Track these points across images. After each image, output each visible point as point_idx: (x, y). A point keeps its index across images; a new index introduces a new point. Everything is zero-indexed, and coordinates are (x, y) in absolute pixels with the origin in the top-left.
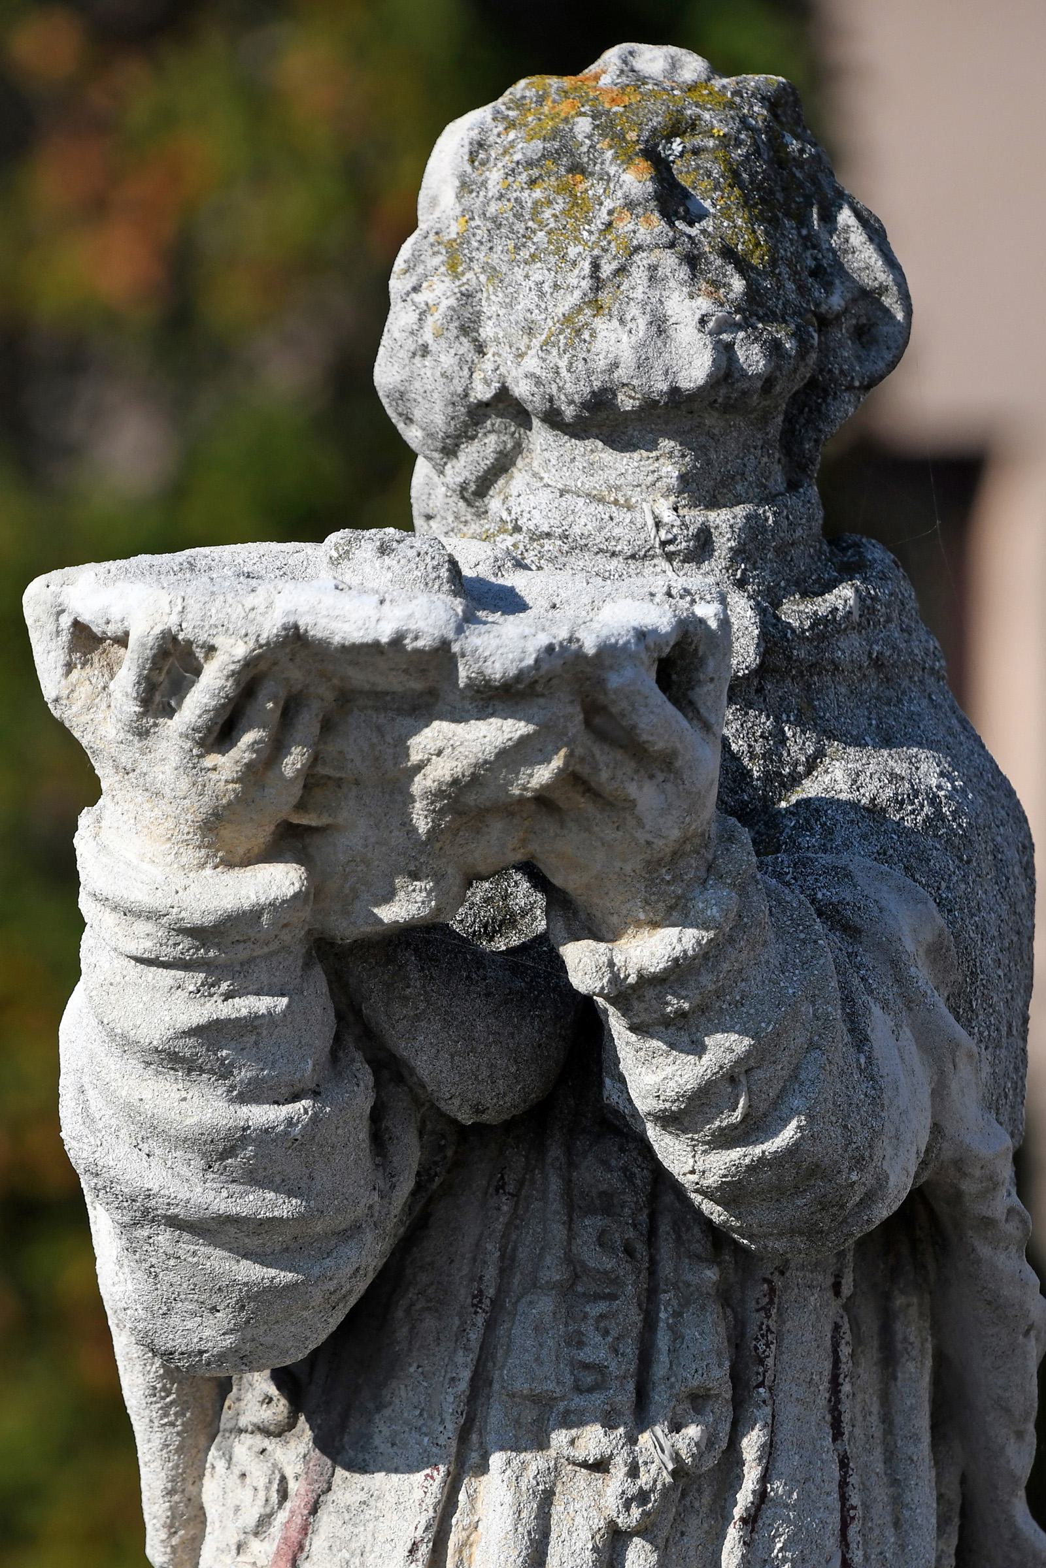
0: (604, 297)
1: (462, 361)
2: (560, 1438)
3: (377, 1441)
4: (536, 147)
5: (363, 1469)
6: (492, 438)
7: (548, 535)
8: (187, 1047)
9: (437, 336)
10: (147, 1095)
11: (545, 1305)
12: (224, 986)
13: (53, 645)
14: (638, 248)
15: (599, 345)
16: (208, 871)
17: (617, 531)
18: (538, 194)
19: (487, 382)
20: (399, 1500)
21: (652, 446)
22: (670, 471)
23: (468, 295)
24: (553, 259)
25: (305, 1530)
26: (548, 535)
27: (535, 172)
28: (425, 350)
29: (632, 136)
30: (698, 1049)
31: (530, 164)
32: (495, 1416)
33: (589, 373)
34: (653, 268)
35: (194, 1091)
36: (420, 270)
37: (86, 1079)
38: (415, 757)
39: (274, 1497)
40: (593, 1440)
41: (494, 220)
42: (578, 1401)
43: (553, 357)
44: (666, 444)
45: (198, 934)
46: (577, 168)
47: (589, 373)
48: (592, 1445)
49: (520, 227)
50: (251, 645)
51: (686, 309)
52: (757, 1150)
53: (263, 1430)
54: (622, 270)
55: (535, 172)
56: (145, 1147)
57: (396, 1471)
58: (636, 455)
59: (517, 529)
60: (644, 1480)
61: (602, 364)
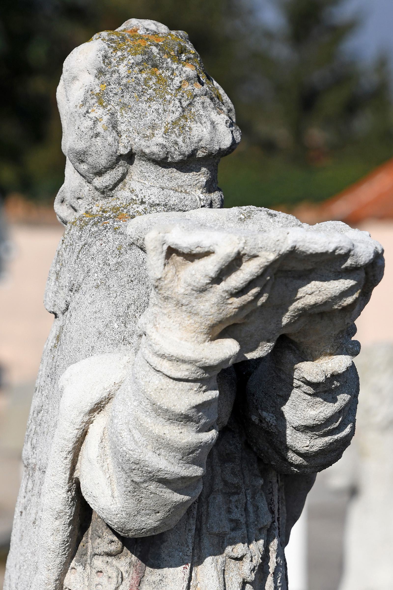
0: (186, 113)
1: (115, 139)
2: (229, 549)
3: (163, 555)
4: (139, 58)
6: (121, 168)
7: (158, 205)
8: (192, 413)
9: (105, 130)
10: (166, 432)
11: (220, 499)
12: (204, 388)
13: (160, 257)
14: (196, 96)
15: (195, 132)
16: (206, 343)
17: (186, 203)
18: (144, 75)
19: (125, 147)
21: (198, 170)
22: (203, 179)
23: (112, 114)
24: (161, 100)
26: (158, 205)
27: (141, 67)
28: (97, 135)
29: (172, 53)
30: (334, 400)
31: (138, 64)
32: (206, 542)
33: (191, 143)
34: (203, 103)
35: (184, 430)
36: (88, 105)
37: (131, 426)
38: (299, 295)
39: (120, 579)
40: (239, 549)
41: (125, 85)
42: (233, 534)
43: (173, 137)
44: (204, 169)
45: (206, 369)
46: (155, 66)
47: (191, 143)
48: (239, 550)
49: (140, 88)
50: (276, 254)
51: (221, 119)
54: (190, 104)
56: (158, 452)
57: (171, 567)
58: (191, 174)
59: (142, 203)
60: (254, 562)
61: (196, 140)
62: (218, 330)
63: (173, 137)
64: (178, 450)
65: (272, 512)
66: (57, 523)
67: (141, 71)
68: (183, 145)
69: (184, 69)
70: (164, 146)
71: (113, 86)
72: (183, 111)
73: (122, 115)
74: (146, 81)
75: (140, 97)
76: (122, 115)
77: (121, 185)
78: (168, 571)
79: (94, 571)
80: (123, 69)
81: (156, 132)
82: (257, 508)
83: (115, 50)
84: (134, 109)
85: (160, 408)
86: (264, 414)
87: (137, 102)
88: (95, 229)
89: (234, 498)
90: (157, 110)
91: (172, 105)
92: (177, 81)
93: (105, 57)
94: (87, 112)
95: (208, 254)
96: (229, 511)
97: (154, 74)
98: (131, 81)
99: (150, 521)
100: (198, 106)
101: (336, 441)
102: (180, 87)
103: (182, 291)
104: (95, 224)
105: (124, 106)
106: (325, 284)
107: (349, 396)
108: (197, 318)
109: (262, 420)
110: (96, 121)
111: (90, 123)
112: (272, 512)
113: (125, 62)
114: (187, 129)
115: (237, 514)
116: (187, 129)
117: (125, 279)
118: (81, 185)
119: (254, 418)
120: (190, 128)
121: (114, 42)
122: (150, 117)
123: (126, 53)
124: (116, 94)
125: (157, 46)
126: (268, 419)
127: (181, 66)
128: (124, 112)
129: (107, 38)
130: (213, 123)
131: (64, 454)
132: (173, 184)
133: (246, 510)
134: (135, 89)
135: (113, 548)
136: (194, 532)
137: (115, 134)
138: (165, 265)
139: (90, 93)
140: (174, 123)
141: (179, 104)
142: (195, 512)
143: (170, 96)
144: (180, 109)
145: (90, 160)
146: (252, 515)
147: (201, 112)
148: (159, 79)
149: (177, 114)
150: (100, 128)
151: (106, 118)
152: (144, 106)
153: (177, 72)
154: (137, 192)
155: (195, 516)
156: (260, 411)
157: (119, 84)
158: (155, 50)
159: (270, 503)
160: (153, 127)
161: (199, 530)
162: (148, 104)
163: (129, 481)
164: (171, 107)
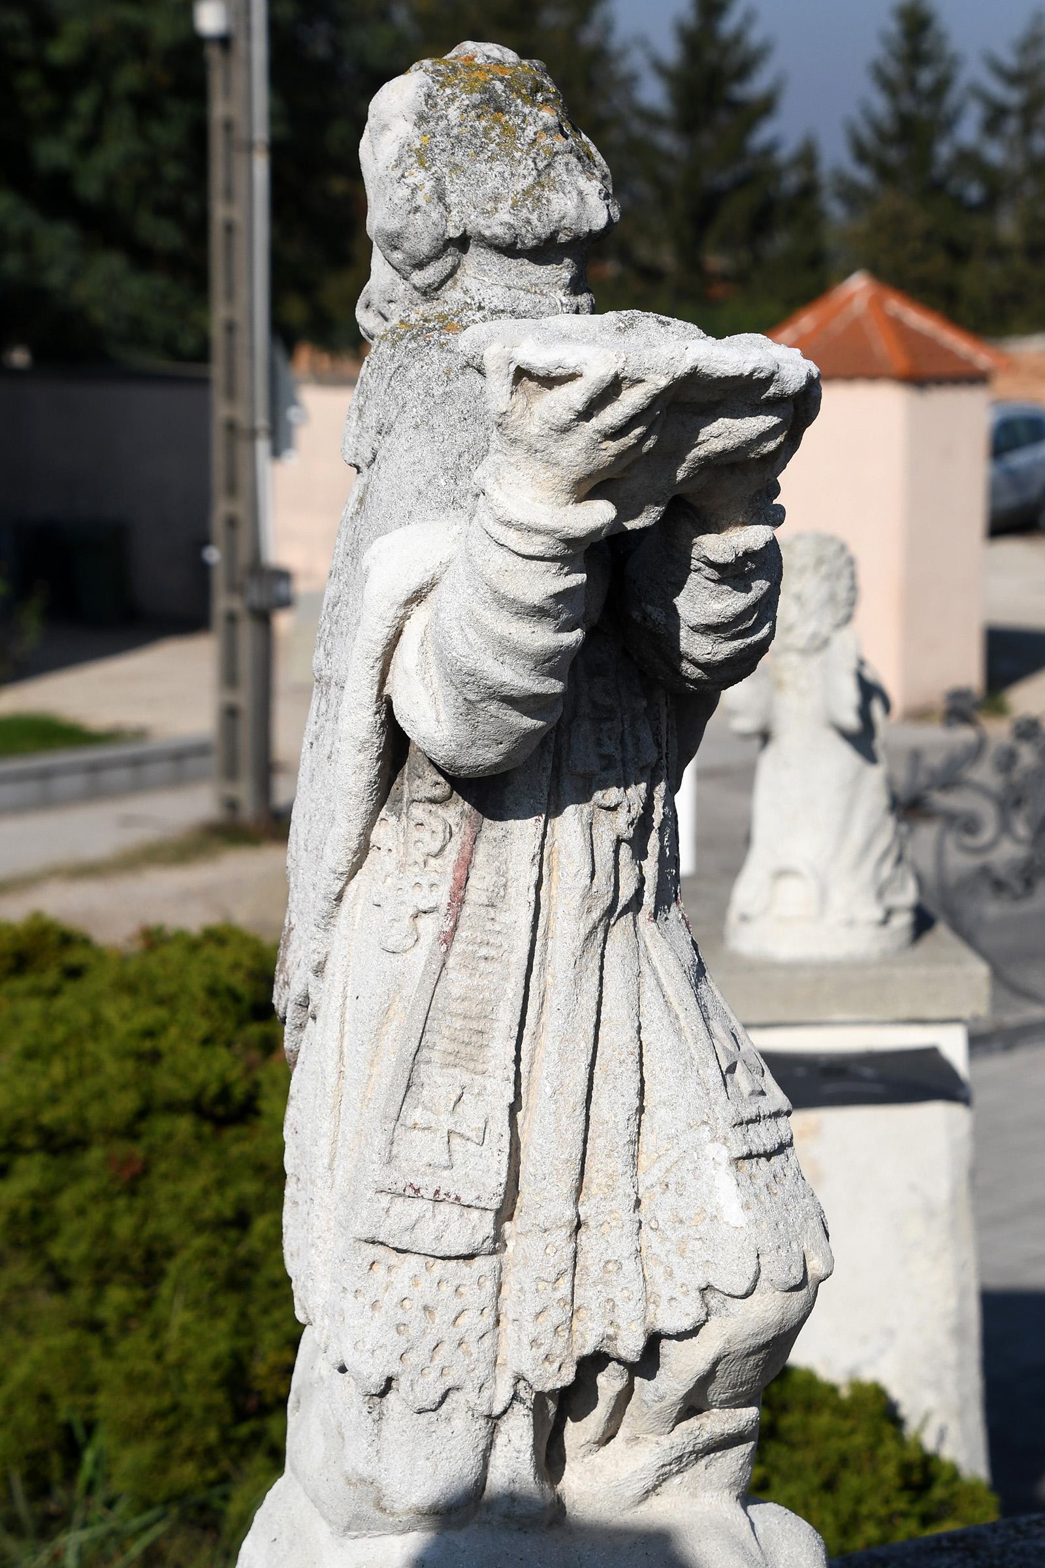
0: (542, 179)
1: (442, 216)
2: (598, 795)
5: (501, 819)
6: (450, 258)
7: (503, 311)
8: (548, 604)
9: (428, 202)
10: (513, 631)
11: (586, 726)
12: (566, 569)
13: (505, 382)
14: (557, 153)
15: (555, 206)
16: (570, 506)
17: (542, 309)
18: (484, 123)
19: (456, 227)
20: (523, 832)
21: (560, 262)
23: (438, 179)
24: (507, 159)
25: (471, 853)
26: (503, 311)
27: (479, 111)
28: (417, 209)
29: (524, 91)
30: (747, 589)
31: (475, 107)
32: (567, 786)
33: (550, 221)
34: (567, 164)
35: (538, 629)
36: (403, 165)
37: (463, 623)
38: (700, 439)
39: (448, 835)
40: (612, 795)
41: (457, 137)
42: (604, 775)
43: (524, 213)
44: (567, 261)
45: (570, 542)
46: (499, 109)
47: (550, 221)
48: (613, 797)
50: (669, 378)
51: (592, 188)
52: (748, 641)
53: (432, 801)
54: (549, 165)
55: (479, 111)
56: (501, 659)
57: (518, 818)
58: (549, 267)
59: (480, 308)
60: (633, 813)
61: (556, 217)
62: (587, 487)
63: (524, 213)
64: (528, 656)
65: (659, 745)
66: (361, 757)
67: (478, 117)
68: (539, 224)
69: (541, 114)
70: (511, 226)
71: (439, 139)
72: (539, 176)
73: (452, 181)
74: (486, 132)
75: (478, 154)
76: (452, 181)
77: (450, 282)
78: (513, 824)
79: (412, 824)
80: (453, 113)
81: (500, 205)
82: (638, 739)
83: (443, 86)
84: (469, 172)
85: (504, 597)
86: (650, 608)
87: (473, 162)
88: (413, 345)
89: (606, 726)
90: (502, 174)
91: (522, 166)
92: (530, 131)
93: (429, 96)
94: (403, 176)
95: (573, 377)
96: (599, 743)
97: (497, 121)
98: (465, 132)
99: (490, 755)
100: (560, 168)
101: (749, 646)
102: (535, 141)
103: (537, 430)
104: (414, 338)
105: (455, 167)
106: (738, 423)
107: (768, 584)
108: (556, 470)
109: (646, 617)
110: (415, 190)
111: (407, 192)
112: (659, 745)
113: (457, 104)
114: (544, 201)
115: (610, 748)
116: (544, 201)
117: (456, 417)
118: (393, 283)
119: (636, 615)
120: (548, 201)
121: (441, 75)
122: (492, 183)
123: (457, 91)
124: (443, 150)
125: (502, 80)
126: (654, 616)
127: (535, 110)
128: (454, 176)
129: (431, 69)
130: (580, 193)
131: (370, 662)
132: (523, 282)
133: (622, 742)
134: (471, 143)
135: (438, 792)
136: (550, 771)
137: (442, 208)
138: (512, 393)
139: (406, 148)
140: (526, 193)
141: (533, 166)
142: (552, 745)
143: (520, 154)
144: (534, 173)
145: (406, 245)
146: (630, 748)
147: (565, 177)
148: (505, 128)
149: (530, 180)
150: (420, 200)
151: (429, 185)
152: (483, 167)
153: (530, 119)
154: (473, 292)
155: (552, 749)
156: (643, 604)
157: (448, 135)
158: (499, 86)
159: (656, 734)
160: (496, 199)
161: (557, 769)
162: (489, 165)
163: (460, 699)
164: (521, 170)
